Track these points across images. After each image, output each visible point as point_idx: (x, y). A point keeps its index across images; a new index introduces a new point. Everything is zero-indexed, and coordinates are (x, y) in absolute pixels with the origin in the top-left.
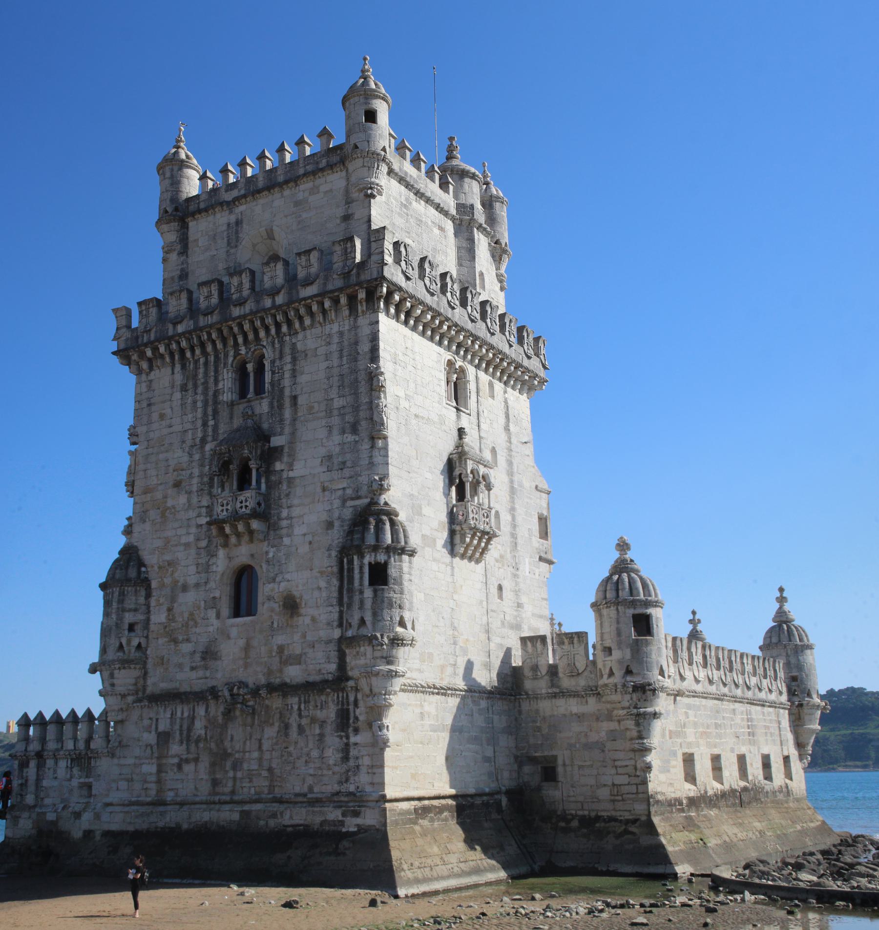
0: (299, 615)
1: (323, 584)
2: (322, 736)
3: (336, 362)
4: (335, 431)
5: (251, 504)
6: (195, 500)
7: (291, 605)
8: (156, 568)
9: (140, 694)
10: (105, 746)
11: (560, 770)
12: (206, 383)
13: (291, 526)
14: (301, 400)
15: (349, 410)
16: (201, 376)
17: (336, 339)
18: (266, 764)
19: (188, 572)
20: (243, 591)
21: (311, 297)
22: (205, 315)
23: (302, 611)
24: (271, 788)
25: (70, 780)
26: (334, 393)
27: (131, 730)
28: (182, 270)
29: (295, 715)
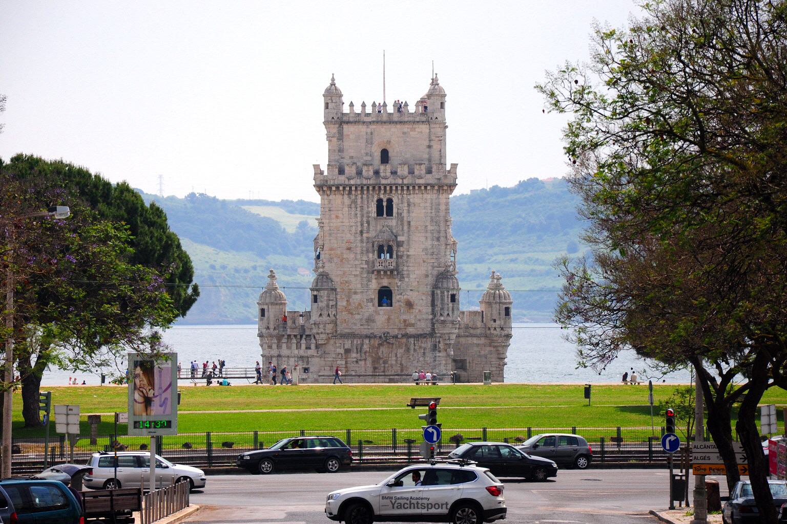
0: (413, 309)
2: (424, 353)
3: (429, 211)
4: (429, 239)
5: (394, 264)
7: (409, 305)
8: (339, 283)
9: (334, 334)
10: (316, 352)
11: (468, 365)
13: (408, 274)
17: (429, 202)
18: (399, 362)
20: (385, 296)
22: (367, 179)
24: (402, 371)
26: (428, 224)
28: (340, 148)
29: (412, 345)
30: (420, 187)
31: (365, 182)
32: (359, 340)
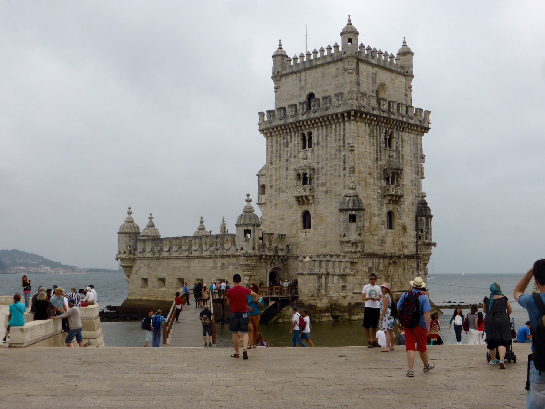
1: (412, 223)
3: (413, 148)
6: (376, 182)
7: (404, 229)
9: (363, 254)
12: (377, 137)
13: (403, 201)
14: (405, 157)
15: (416, 166)
16: (375, 133)
19: (374, 209)
21: (413, 124)
22: (383, 112)
23: (407, 231)
24: (401, 287)
25: (339, 283)
26: (412, 159)
27: (359, 266)
30: (411, 126)
31: (382, 114)
32: (377, 259)
